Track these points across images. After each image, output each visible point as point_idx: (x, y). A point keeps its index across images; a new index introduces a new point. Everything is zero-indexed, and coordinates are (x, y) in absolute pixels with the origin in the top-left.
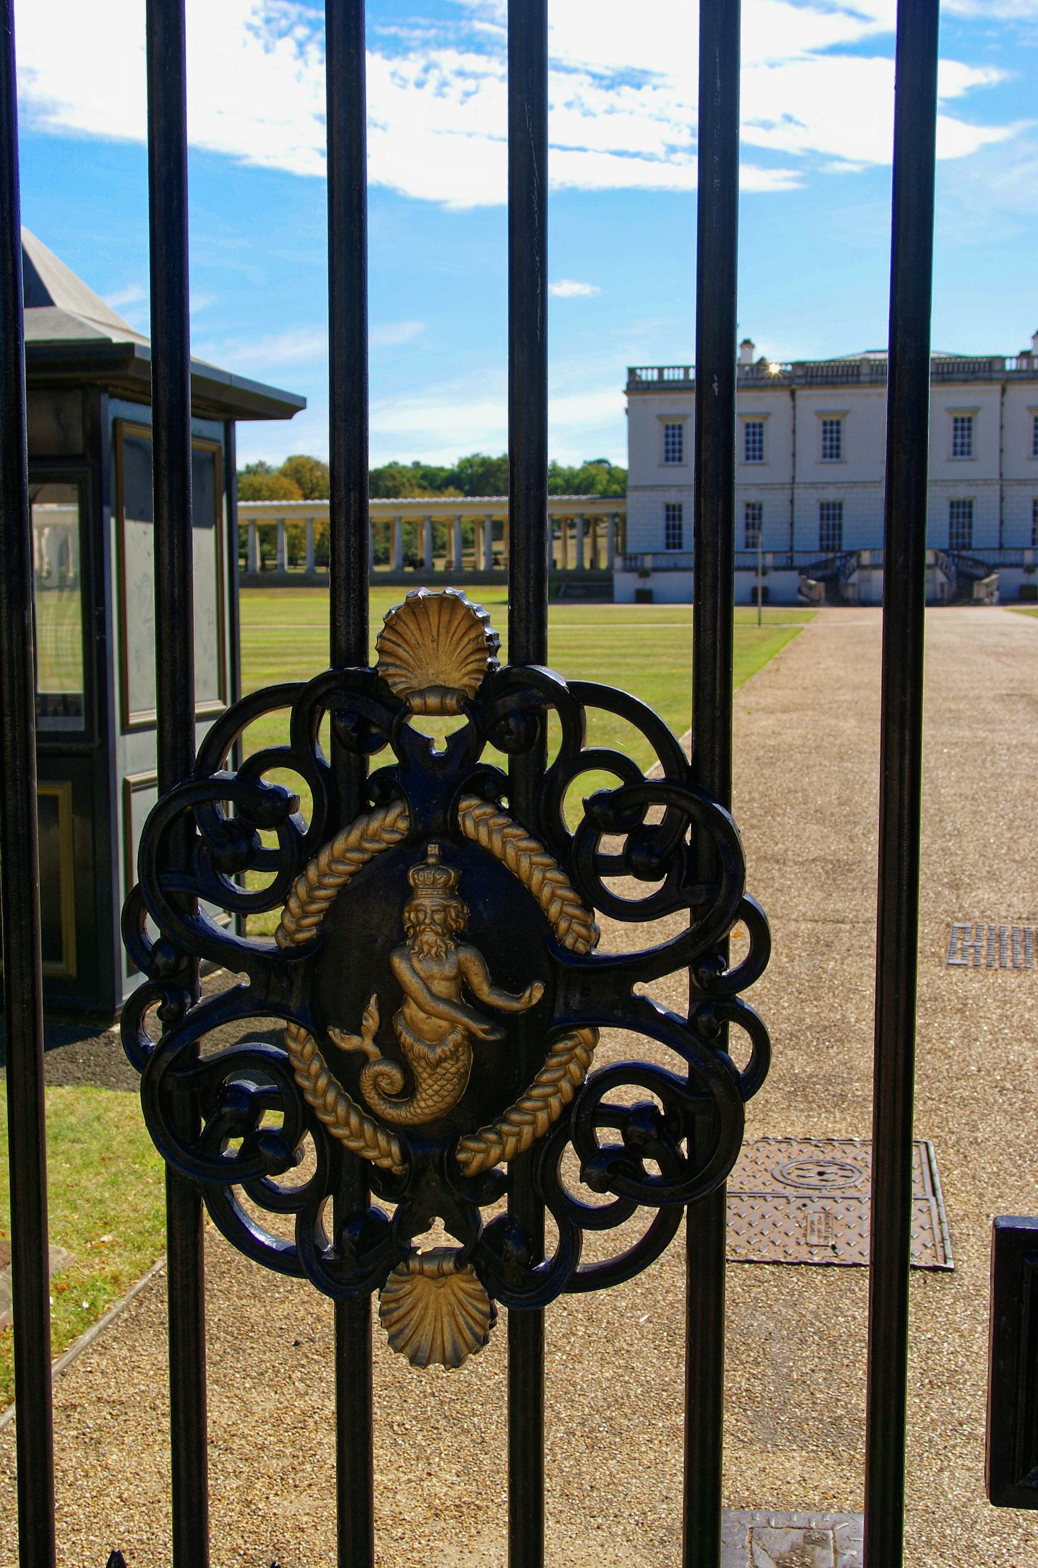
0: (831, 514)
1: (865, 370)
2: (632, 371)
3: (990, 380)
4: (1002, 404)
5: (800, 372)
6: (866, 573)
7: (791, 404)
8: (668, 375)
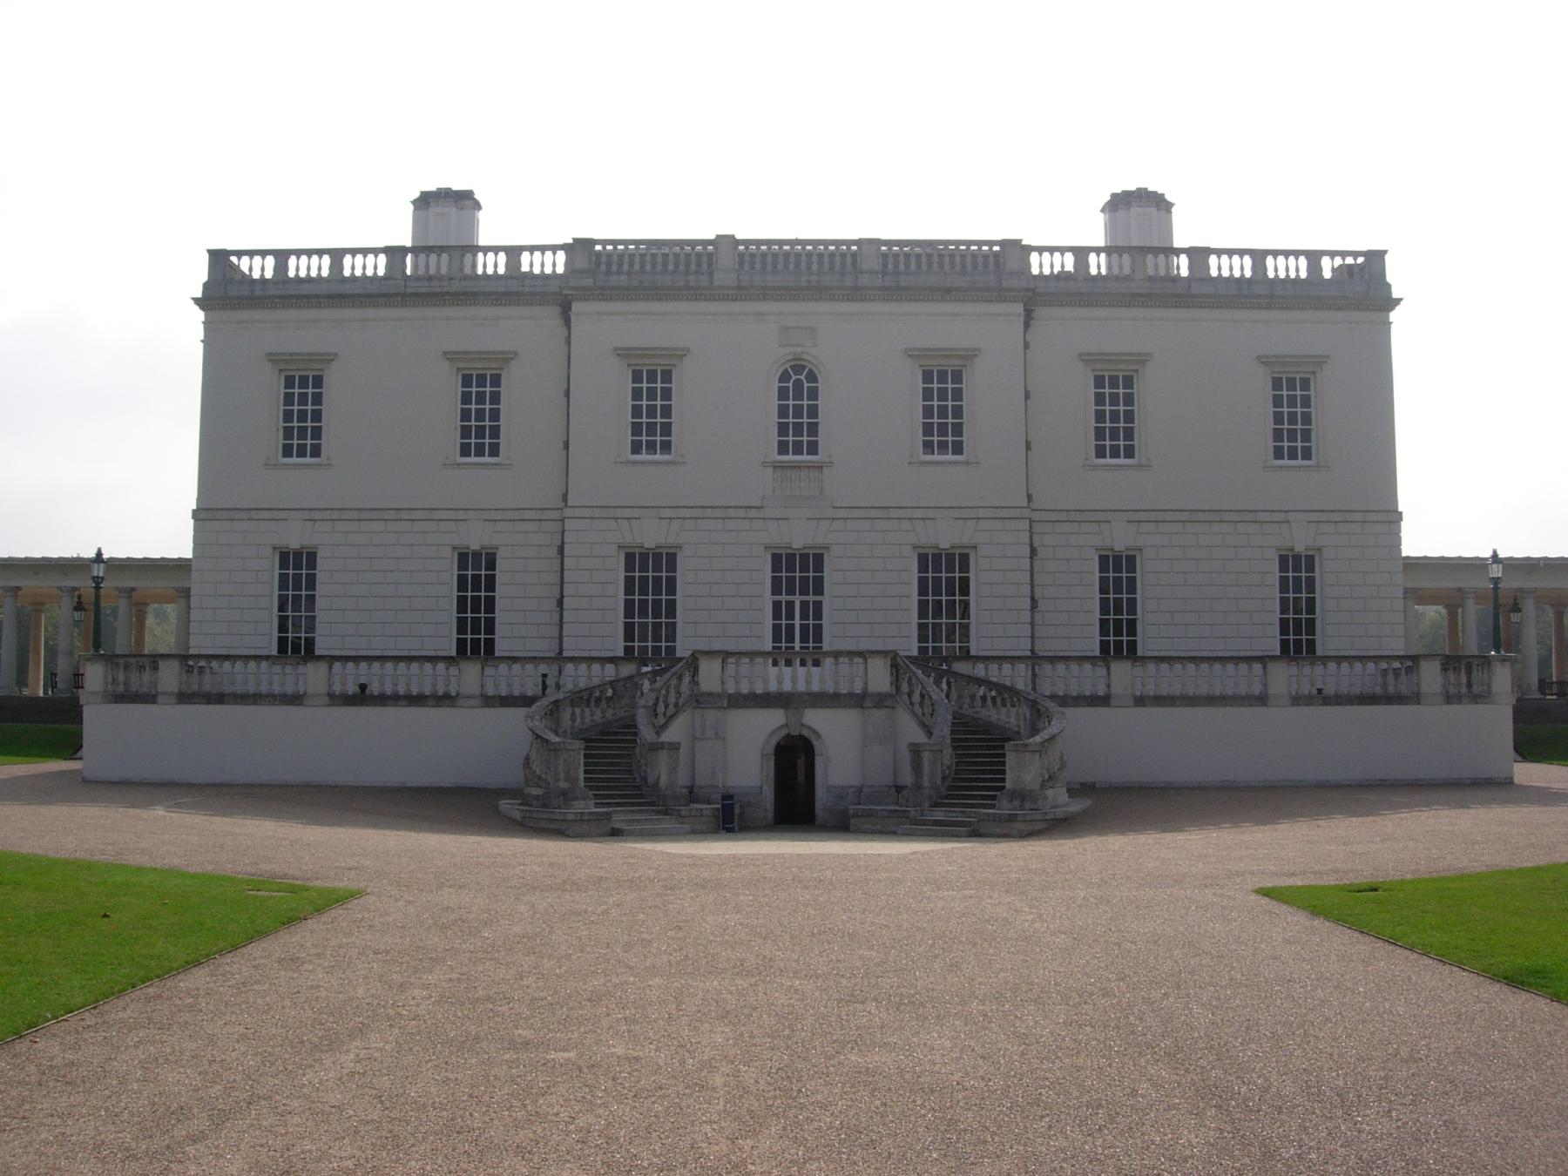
0: (651, 579)
1: (725, 261)
2: (219, 259)
3: (1000, 294)
4: (1026, 346)
5: (582, 263)
6: (711, 715)
7: (563, 332)
8: (298, 268)
